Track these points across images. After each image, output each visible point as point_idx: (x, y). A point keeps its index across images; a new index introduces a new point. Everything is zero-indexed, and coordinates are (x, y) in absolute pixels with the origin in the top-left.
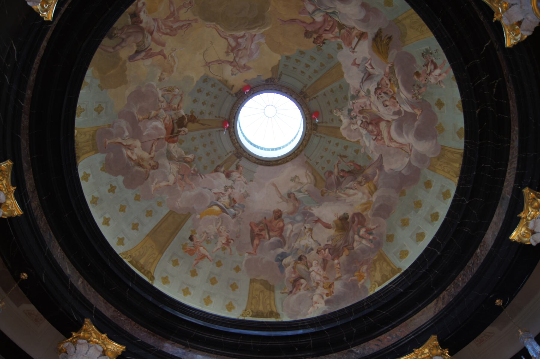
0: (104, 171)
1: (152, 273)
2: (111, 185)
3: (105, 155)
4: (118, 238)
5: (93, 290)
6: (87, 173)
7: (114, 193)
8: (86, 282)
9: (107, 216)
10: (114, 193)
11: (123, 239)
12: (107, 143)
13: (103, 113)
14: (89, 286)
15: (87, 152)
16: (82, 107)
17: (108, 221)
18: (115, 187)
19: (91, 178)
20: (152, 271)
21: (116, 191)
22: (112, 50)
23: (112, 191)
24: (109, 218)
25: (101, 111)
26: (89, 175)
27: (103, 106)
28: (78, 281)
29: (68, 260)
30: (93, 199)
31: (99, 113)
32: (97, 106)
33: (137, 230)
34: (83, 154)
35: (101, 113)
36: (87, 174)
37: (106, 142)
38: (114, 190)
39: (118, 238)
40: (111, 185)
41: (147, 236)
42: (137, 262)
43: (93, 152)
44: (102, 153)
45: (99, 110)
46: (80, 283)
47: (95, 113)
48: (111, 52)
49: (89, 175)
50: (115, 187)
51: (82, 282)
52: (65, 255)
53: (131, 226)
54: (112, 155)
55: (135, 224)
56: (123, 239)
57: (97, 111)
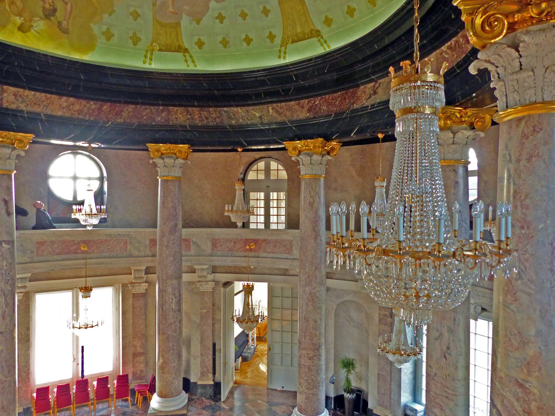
0: (199, 21)
1: (314, 28)
2: (217, 18)
3: (184, 16)
4: (267, 37)
5: (284, 104)
6: (197, 40)
7: (225, 18)
8: (275, 105)
9: (243, 36)
10: (225, 18)
11: (270, 33)
12: (172, 10)
13: (139, 11)
14: (279, 105)
15: (177, 35)
16: (132, 35)
17: (249, 38)
18: (220, 14)
19: (203, 39)
20: (312, 28)
21: (223, 15)
22: (69, 5)
23: (223, 20)
24: (247, 35)
25: (137, 13)
26: (199, 39)
27: (132, 10)
28: (269, 112)
29: (251, 108)
30: (223, 44)
31: (139, 15)
32: (131, 17)
33: (269, 11)
34: (178, 40)
35: (139, 13)
36: (198, 42)
37: (171, 12)
38: (222, 16)
39: (267, 37)
40: (217, 18)
41: (280, 5)
42: (297, 35)
43: (178, 28)
44: (181, 19)
45: (136, 15)
46: (271, 112)
47: (139, 20)
48: (72, 5)
49: (199, 39)
50: (220, 14)
51: (272, 109)
52: (246, 108)
53: (264, 16)
54: (186, 7)
55: (264, 10)
56: (270, 33)
57: (137, 18)
